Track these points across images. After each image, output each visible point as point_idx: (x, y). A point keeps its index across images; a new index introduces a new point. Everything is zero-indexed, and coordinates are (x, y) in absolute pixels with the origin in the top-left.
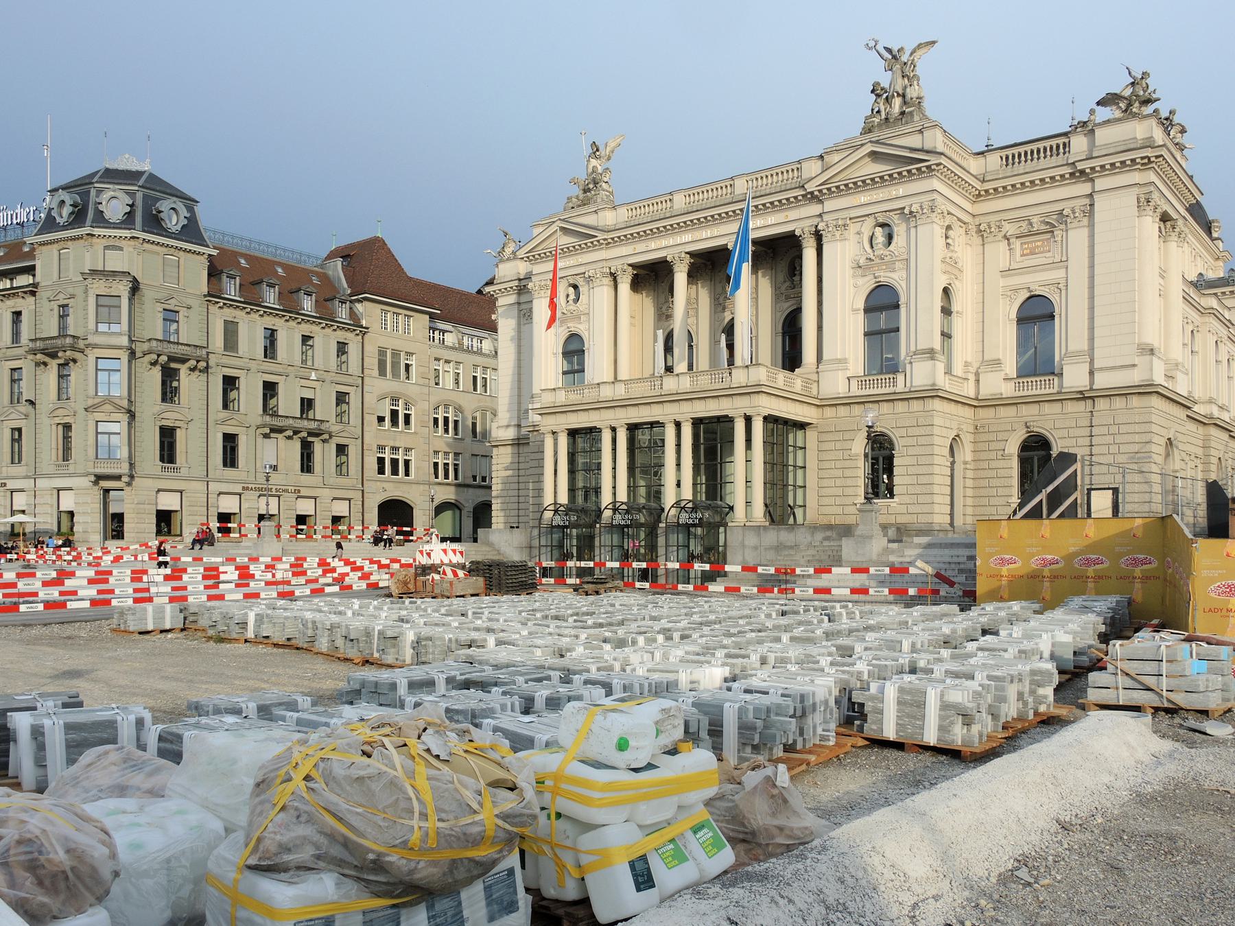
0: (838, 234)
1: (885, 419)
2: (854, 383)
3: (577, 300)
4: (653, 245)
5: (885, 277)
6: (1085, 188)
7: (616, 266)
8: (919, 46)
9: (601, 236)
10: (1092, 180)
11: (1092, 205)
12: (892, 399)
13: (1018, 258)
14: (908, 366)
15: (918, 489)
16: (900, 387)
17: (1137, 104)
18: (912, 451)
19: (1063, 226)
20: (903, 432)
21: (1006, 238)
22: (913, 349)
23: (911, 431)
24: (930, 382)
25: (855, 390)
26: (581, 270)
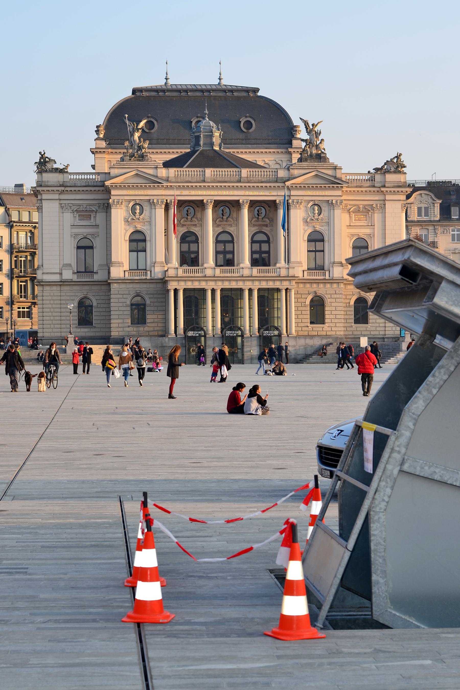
0: (297, 206)
1: (321, 290)
2: (305, 273)
3: (141, 214)
4: (193, 193)
5: (318, 228)
6: (382, 198)
7: (169, 199)
8: (319, 123)
9: (165, 184)
10: (385, 195)
11: (385, 205)
12: (325, 282)
13: (354, 221)
14: (331, 269)
15: (336, 321)
16: (327, 277)
17: (400, 167)
18: (333, 304)
19: (372, 211)
20: (329, 296)
21: (349, 211)
22: (332, 261)
23: (333, 296)
24: (341, 276)
25: (306, 277)
26: (148, 198)
